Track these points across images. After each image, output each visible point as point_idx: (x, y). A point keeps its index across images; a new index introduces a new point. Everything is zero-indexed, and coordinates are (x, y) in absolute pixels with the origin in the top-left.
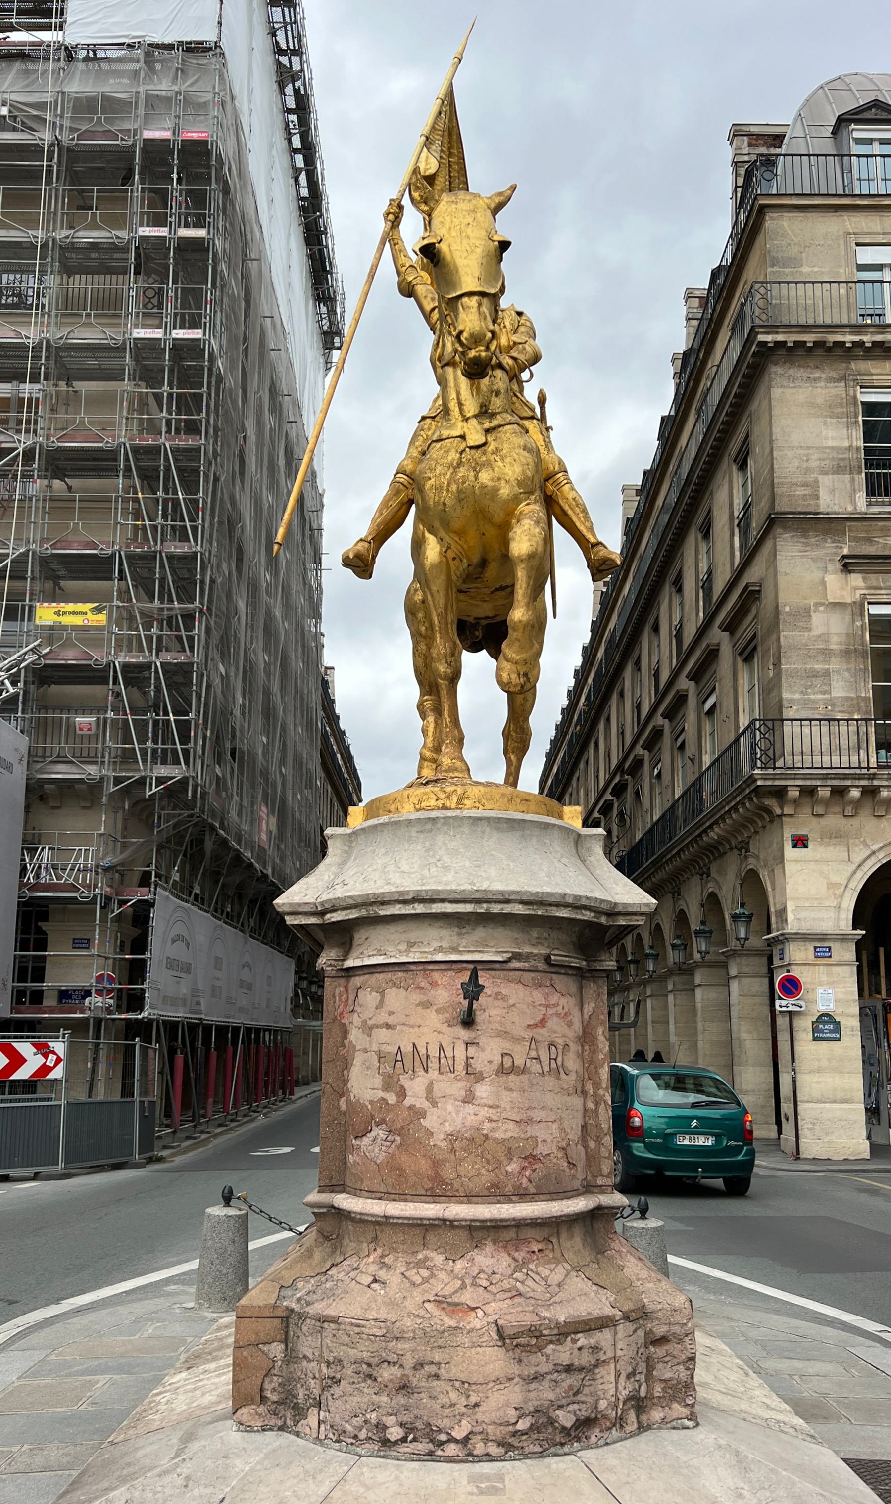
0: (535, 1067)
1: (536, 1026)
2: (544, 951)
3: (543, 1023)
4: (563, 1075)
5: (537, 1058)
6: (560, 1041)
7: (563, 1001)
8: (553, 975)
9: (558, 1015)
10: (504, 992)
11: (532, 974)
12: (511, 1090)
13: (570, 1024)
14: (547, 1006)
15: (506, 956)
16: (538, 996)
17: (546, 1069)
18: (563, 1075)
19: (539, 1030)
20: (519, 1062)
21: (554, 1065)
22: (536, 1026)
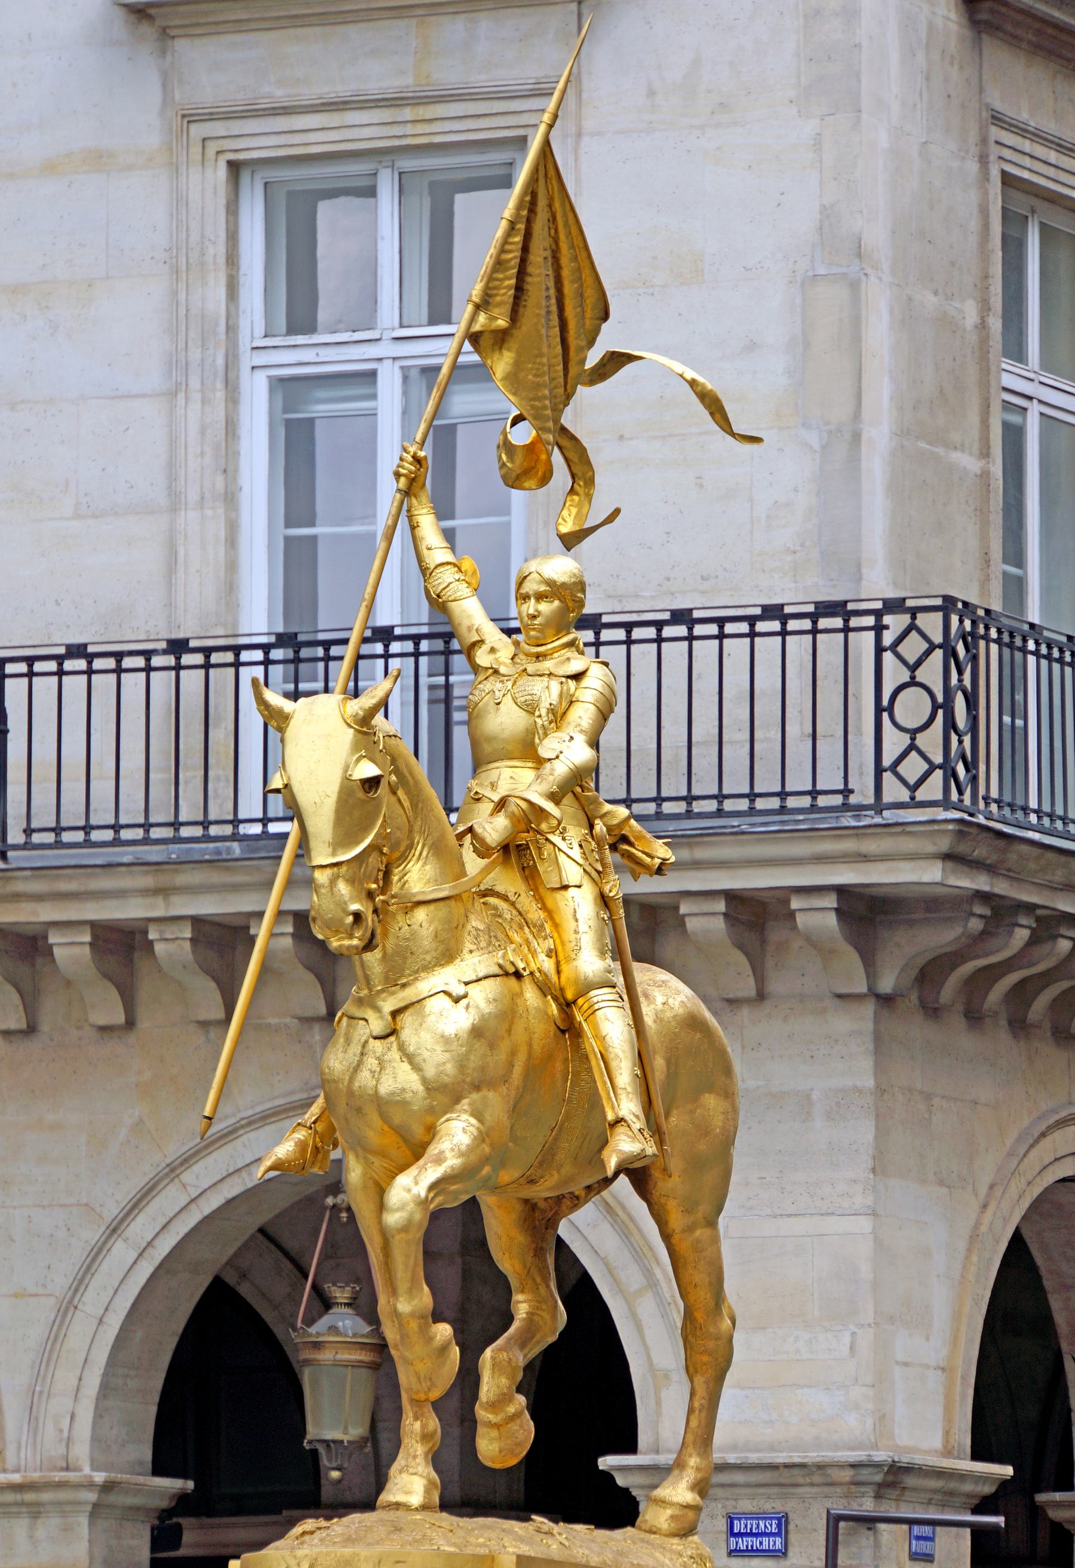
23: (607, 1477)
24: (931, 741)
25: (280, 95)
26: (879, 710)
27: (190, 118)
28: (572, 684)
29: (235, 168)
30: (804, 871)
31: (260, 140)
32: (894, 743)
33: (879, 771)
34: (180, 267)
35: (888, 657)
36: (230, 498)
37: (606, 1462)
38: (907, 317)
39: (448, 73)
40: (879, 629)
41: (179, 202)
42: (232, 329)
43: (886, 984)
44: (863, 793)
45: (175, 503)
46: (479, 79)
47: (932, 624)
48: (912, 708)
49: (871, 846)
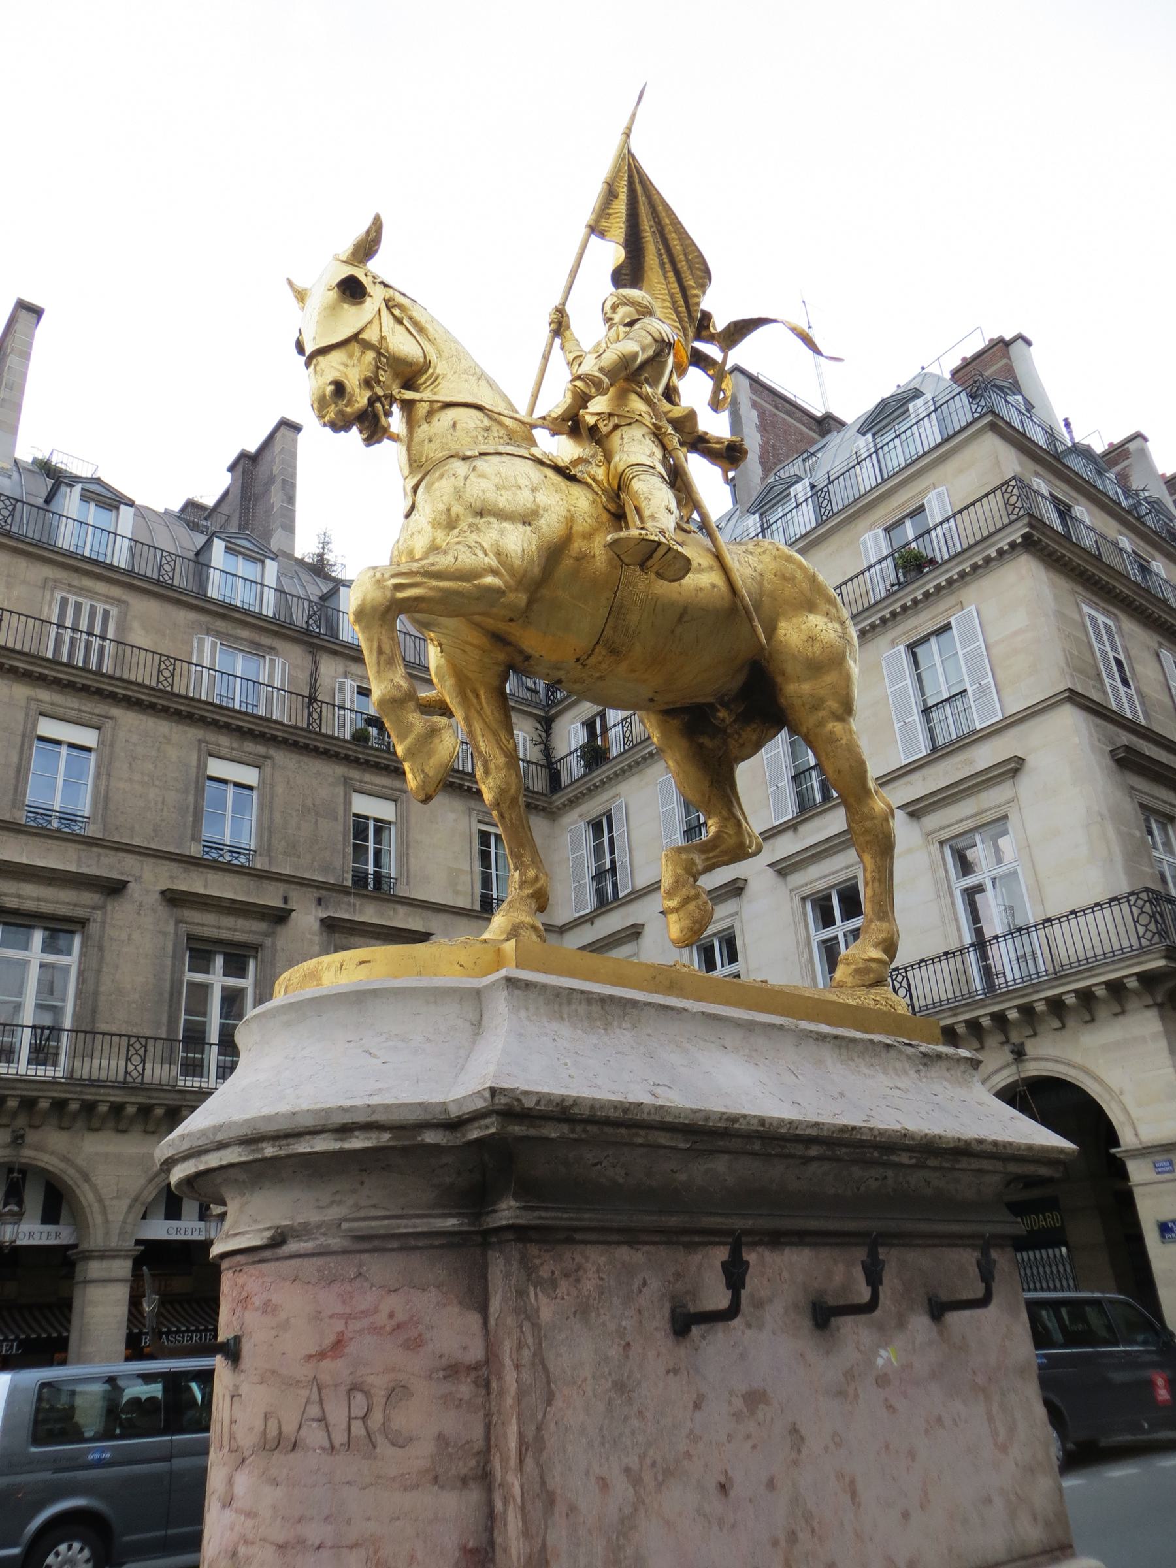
0: (314, 1436)
1: (322, 1355)
2: (334, 1213)
3: (338, 1346)
4: (384, 1448)
5: (323, 1419)
6: (379, 1383)
7: (393, 1302)
8: (366, 1256)
9: (375, 1330)
10: (275, 1298)
11: (319, 1261)
12: (275, 1482)
13: (415, 1344)
14: (348, 1318)
15: (268, 1234)
16: (330, 1300)
17: (339, 1438)
18: (384, 1448)
19: (325, 1363)
20: (289, 1429)
21: (358, 1429)
22: (322, 1355)
23: (1113, 1156)
24: (1152, 927)
25: (947, 823)
26: (1135, 922)
27: (928, 835)
28: (628, 329)
29: (942, 843)
30: (1125, 971)
31: (945, 835)
32: (1141, 930)
33: (1139, 938)
34: (933, 869)
35: (1134, 908)
36: (956, 919)
37: (1113, 1150)
38: (1119, 832)
39: (985, 806)
40: (1129, 901)
41: (930, 854)
42: (948, 880)
43: (1159, 1000)
44: (1136, 945)
45: (944, 923)
46: (993, 804)
47: (1144, 896)
48: (1144, 919)
49: (1142, 959)
